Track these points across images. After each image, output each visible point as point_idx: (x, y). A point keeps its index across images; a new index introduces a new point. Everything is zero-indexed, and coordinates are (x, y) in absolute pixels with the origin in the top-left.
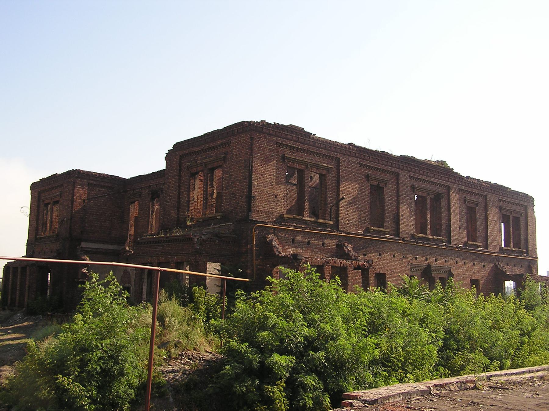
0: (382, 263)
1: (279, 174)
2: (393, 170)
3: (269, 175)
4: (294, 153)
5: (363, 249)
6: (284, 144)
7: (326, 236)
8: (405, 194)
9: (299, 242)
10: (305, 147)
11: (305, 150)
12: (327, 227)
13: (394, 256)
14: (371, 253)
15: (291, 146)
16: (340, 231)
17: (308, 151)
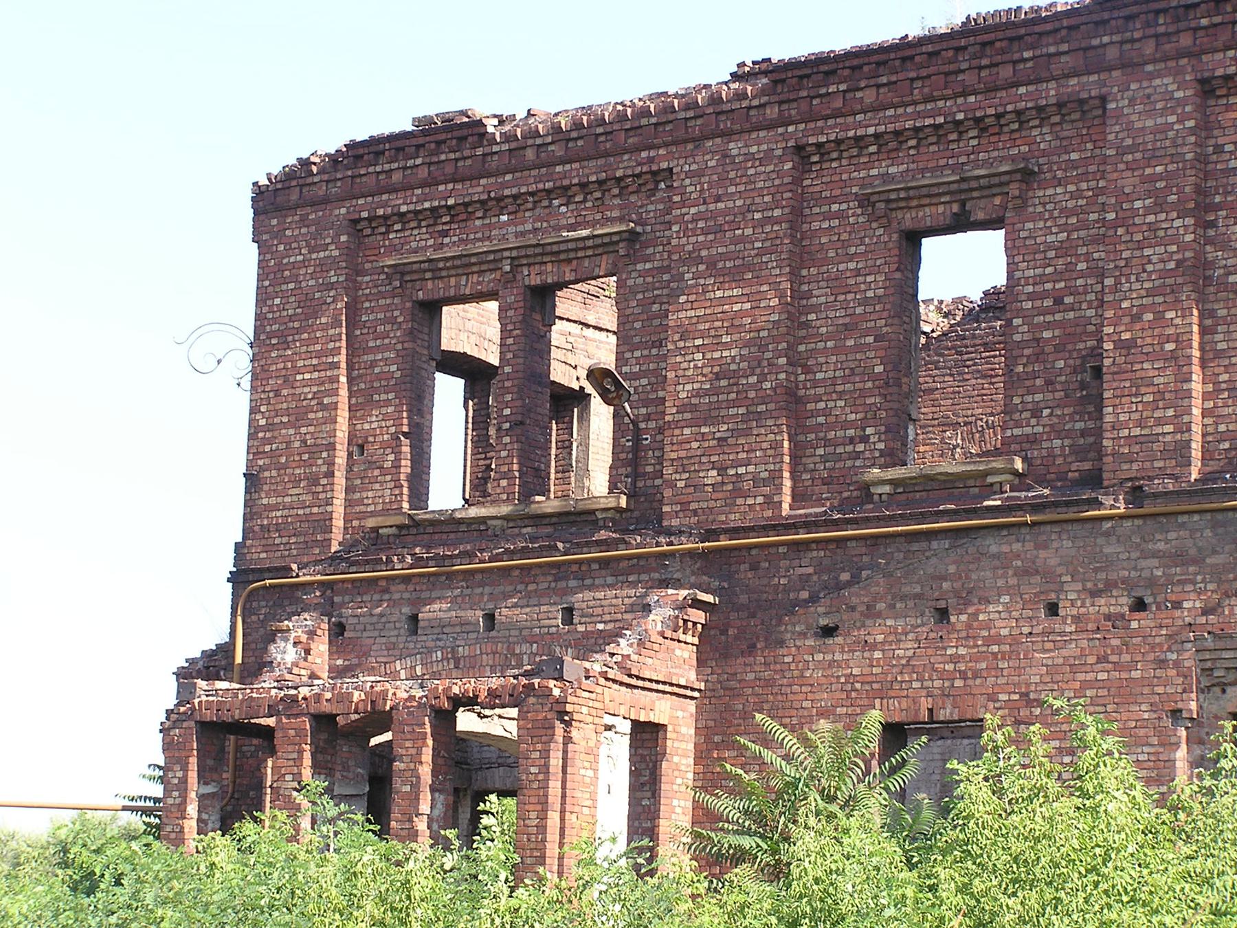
0: (955, 659)
1: (377, 349)
2: (1050, 92)
3: (315, 369)
4: (445, 234)
5: (814, 599)
6: (385, 217)
7: (584, 574)
8: (1160, 207)
9: (441, 626)
10: (477, 191)
11: (483, 202)
12: (596, 525)
13: (1053, 609)
14: (871, 613)
15: (416, 212)
16: (669, 532)
17: (499, 199)
